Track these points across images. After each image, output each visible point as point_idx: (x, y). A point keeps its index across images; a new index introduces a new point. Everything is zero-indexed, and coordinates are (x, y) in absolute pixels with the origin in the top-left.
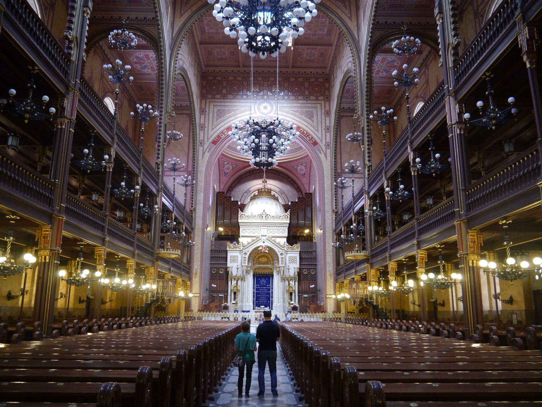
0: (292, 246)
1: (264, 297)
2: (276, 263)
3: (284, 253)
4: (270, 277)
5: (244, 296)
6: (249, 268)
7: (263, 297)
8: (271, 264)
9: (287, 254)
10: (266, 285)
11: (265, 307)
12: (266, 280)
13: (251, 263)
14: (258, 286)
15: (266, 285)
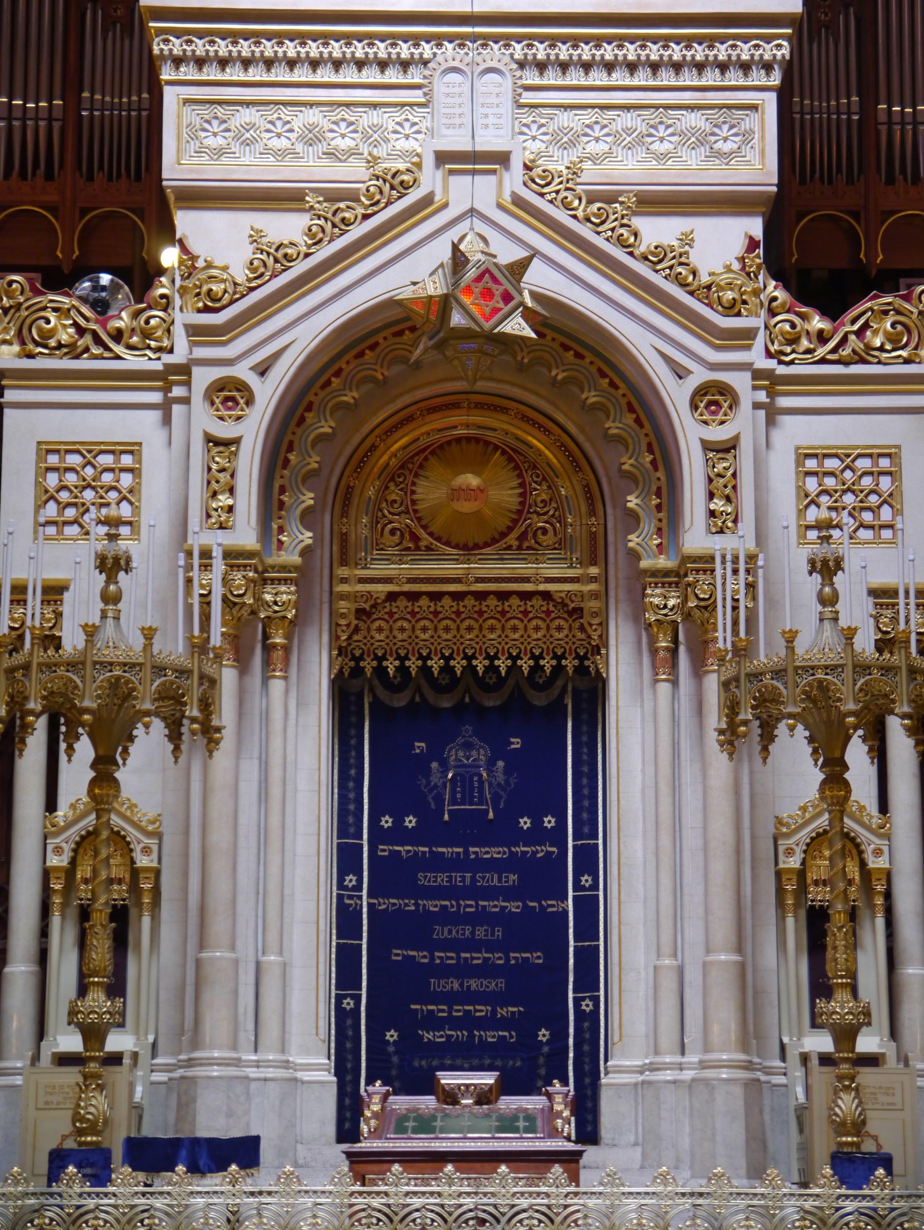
0: (833, 312)
1: (486, 970)
2: (632, 520)
3: (740, 382)
4: (556, 712)
5: (217, 954)
6: (287, 594)
7: (464, 970)
8: (560, 545)
9: (772, 414)
10: (508, 817)
11: (508, 1086)
12: (499, 750)
13: (308, 518)
14: (398, 834)
15: (508, 817)
